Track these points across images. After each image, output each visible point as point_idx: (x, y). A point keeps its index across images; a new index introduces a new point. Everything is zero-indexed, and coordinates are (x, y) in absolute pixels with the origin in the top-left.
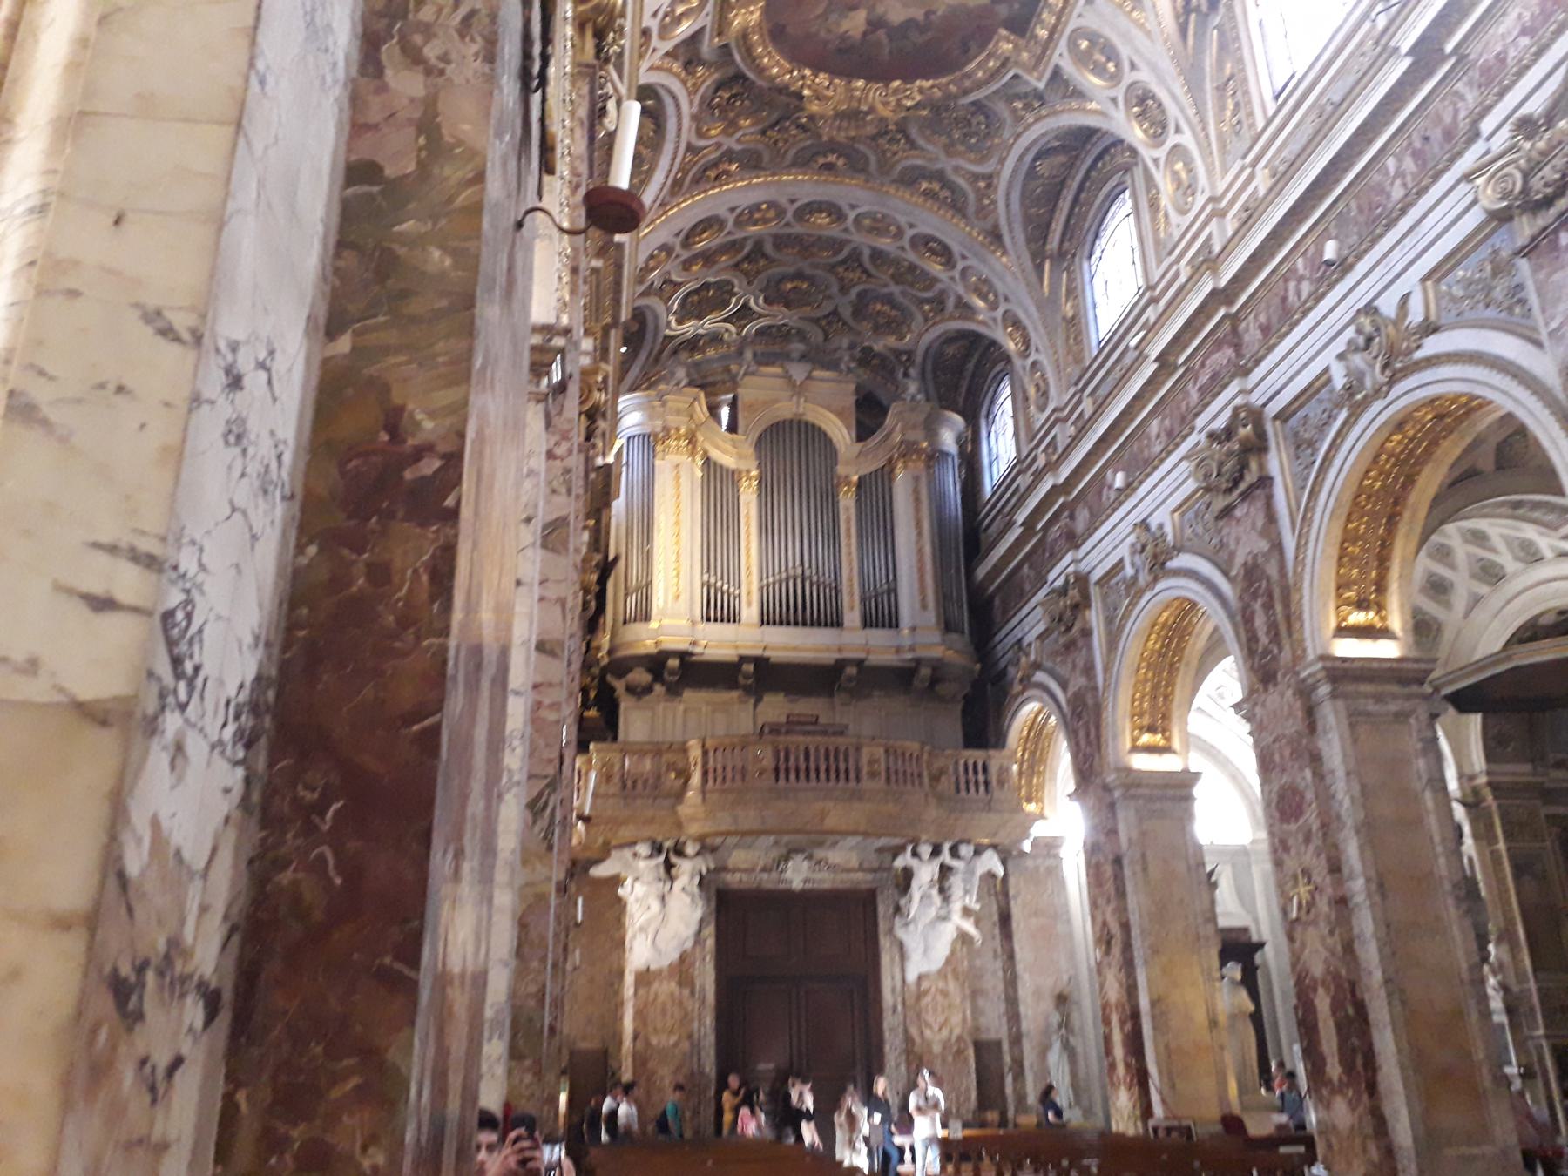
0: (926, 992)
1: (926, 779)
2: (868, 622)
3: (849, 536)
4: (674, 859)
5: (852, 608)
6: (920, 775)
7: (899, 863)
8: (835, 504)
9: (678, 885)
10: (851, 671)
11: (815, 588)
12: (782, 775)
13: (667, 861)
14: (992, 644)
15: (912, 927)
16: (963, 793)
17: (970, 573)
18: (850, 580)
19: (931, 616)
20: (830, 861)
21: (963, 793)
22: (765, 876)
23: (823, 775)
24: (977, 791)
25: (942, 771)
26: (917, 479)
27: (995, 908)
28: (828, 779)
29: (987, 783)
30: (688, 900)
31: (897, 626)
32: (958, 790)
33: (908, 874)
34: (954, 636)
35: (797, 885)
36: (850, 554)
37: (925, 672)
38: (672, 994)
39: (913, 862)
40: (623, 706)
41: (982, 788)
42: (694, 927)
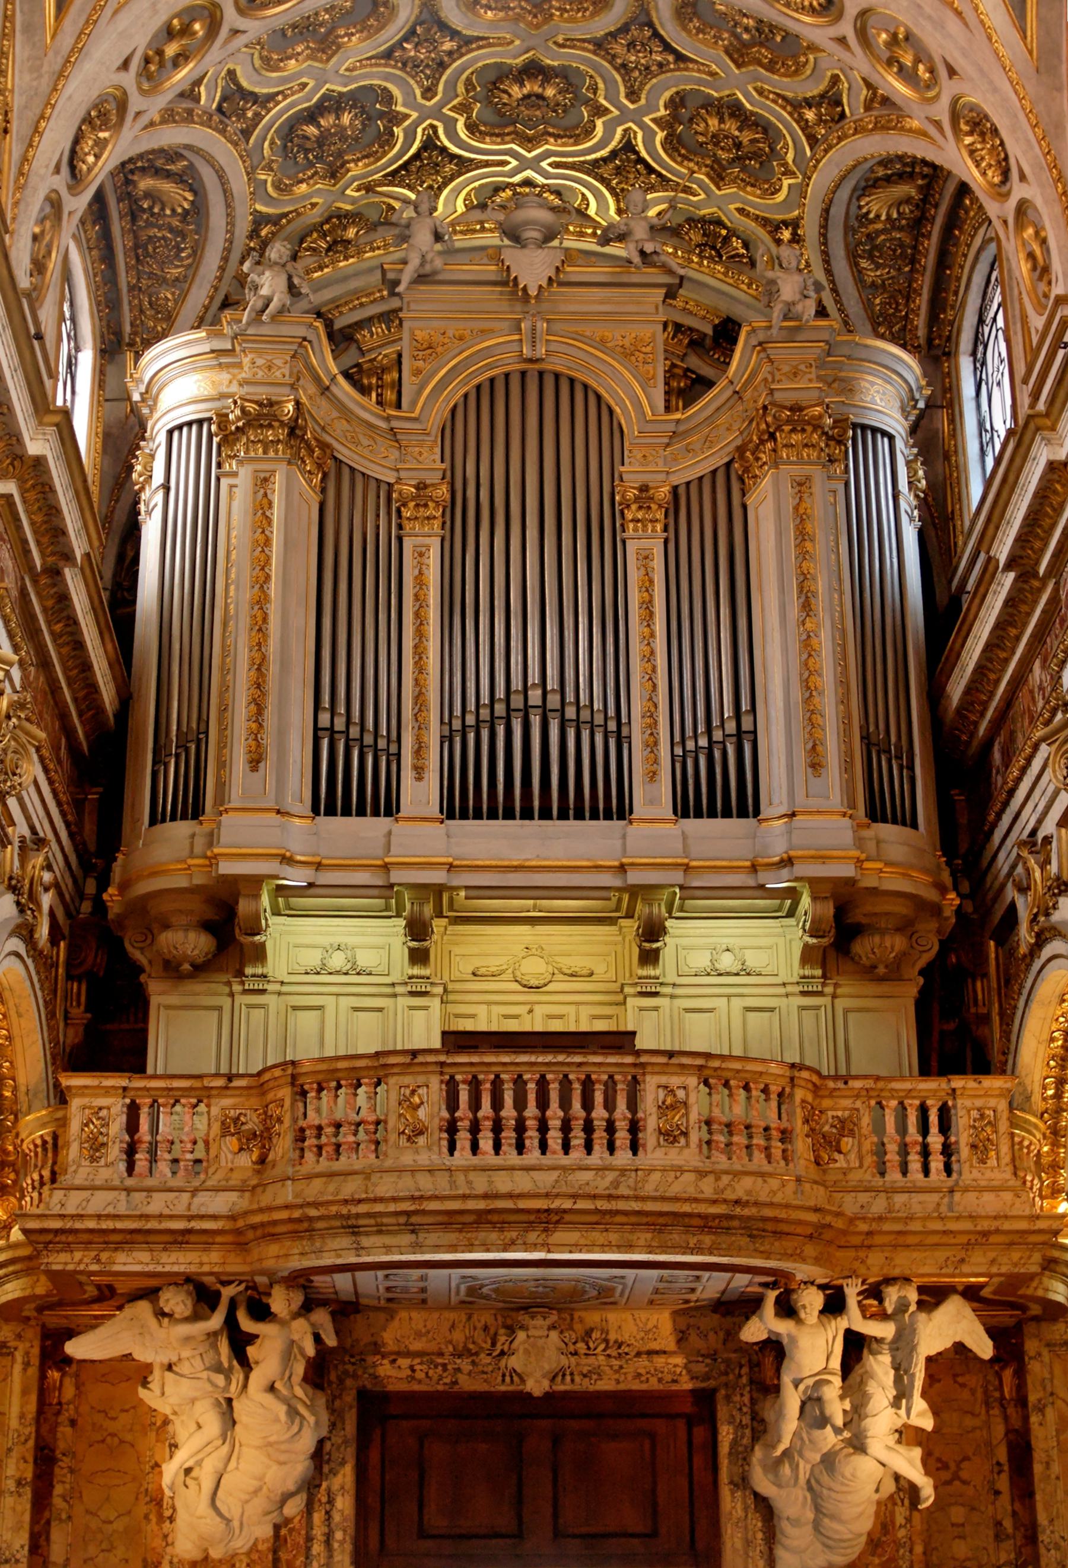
1: (802, 1146)
4: (247, 1324)
5: (653, 776)
6: (786, 1135)
7: (753, 1332)
8: (619, 546)
9: (258, 1378)
11: (571, 734)
12: (463, 1138)
13: (231, 1322)
14: (988, 855)
15: (786, 1470)
16: (894, 1176)
17: (934, 692)
18: (650, 715)
20: (612, 1337)
21: (894, 1176)
22: (465, 1364)
23: (554, 1137)
24: (926, 1171)
25: (846, 1126)
26: (802, 485)
27: (999, 1430)
29: (947, 1150)
30: (281, 1410)
31: (757, 812)
34: (887, 831)
35: (536, 1386)
39: (783, 1327)
40: (154, 1001)
41: (937, 1163)
42: (300, 1467)
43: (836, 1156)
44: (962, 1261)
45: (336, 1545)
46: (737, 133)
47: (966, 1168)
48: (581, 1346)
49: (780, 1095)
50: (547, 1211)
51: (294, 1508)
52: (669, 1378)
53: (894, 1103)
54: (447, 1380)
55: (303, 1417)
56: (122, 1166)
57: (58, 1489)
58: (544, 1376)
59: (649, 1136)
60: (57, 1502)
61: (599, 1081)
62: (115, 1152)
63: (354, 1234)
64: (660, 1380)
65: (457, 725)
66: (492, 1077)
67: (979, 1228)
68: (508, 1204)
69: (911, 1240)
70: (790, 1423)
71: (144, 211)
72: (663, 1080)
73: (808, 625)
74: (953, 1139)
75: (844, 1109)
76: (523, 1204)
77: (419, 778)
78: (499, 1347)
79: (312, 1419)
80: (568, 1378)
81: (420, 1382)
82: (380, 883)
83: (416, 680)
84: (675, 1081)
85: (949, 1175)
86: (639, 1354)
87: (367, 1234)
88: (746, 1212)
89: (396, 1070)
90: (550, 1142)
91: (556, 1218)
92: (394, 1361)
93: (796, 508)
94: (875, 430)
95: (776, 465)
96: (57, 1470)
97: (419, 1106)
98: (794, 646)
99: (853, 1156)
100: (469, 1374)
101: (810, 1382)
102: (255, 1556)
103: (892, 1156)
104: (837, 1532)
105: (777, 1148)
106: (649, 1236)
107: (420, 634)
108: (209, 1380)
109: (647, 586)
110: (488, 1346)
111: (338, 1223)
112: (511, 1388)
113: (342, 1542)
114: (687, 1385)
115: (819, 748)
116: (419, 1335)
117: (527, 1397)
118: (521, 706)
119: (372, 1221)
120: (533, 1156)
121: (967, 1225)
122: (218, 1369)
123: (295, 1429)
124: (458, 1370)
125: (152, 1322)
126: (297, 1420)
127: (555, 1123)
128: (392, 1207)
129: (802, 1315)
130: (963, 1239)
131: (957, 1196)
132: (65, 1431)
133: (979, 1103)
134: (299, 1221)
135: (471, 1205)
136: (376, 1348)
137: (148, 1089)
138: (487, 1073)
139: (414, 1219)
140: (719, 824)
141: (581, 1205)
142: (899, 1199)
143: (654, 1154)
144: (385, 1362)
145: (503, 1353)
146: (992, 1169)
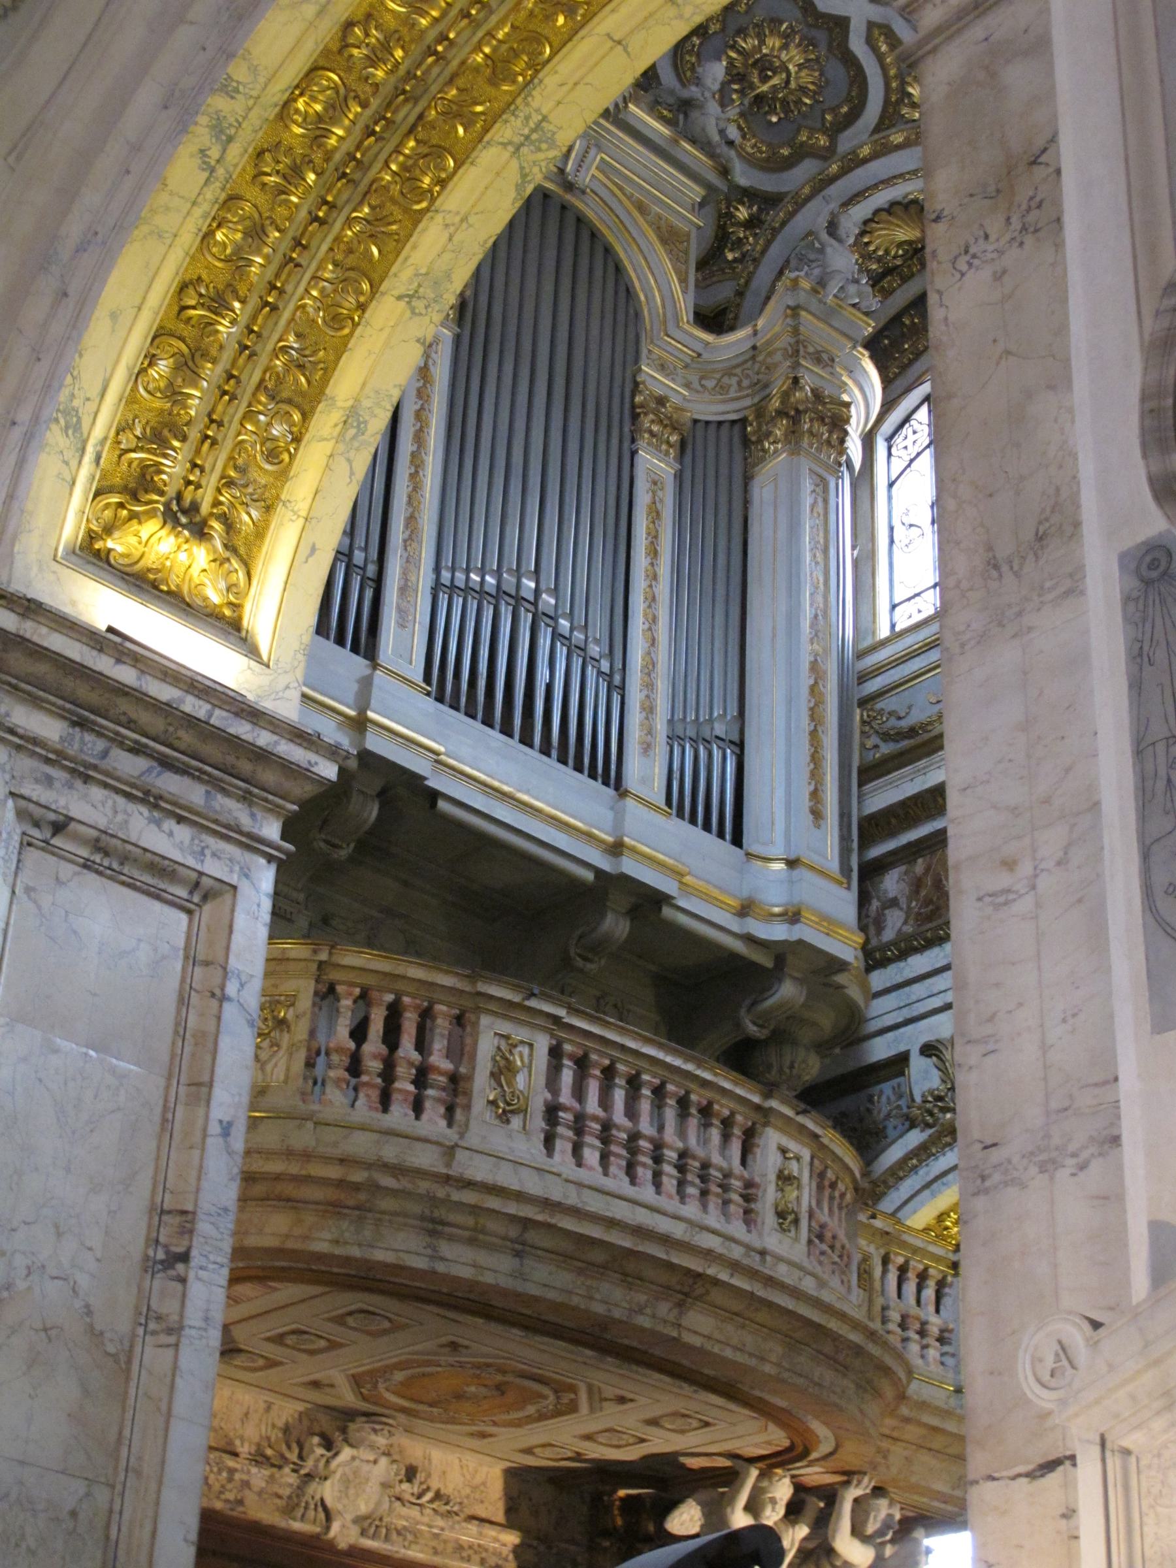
22: (258, 1476)
35: (343, 1533)
36: (652, 600)
37: (788, 991)
50: (699, 1276)
54: (230, 1496)
61: (718, 1114)
63: (433, 1233)
68: (659, 1252)
83: (410, 497)
87: (451, 1238)
89: (493, 1007)
95: (795, 451)
100: (260, 1493)
110: (293, 1456)
111: (417, 1209)
117: (331, 1546)
119: (470, 1221)
124: (246, 1484)
128: (512, 1208)
134: (356, 1187)
138: (602, 1054)
139: (532, 1236)
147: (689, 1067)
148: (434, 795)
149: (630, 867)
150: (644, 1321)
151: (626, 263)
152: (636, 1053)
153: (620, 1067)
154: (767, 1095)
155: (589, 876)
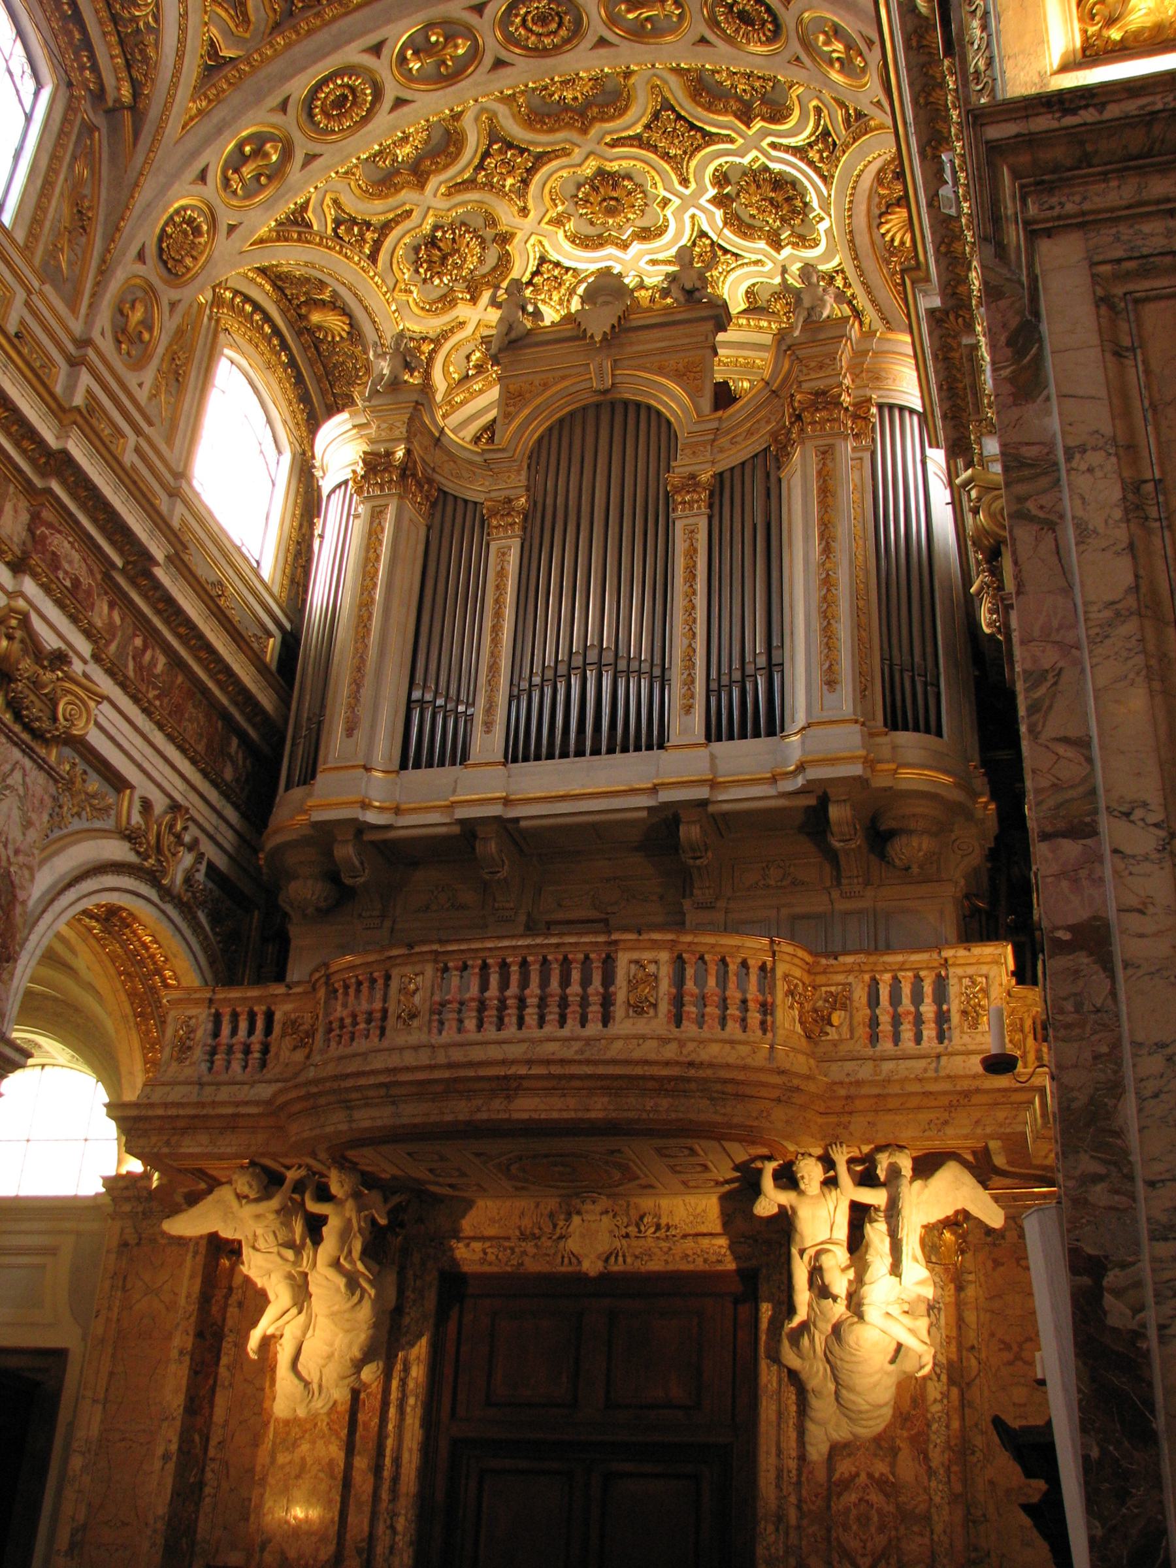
0: (846, 1484)
2: (714, 732)
3: (691, 576)
5: (688, 709)
10: (690, 832)
15: (805, 1341)
16: (886, 1046)
19: (845, 700)
20: (663, 1221)
22: (529, 1247)
23: (531, 1015)
24: (918, 1039)
28: (542, 1022)
29: (942, 1018)
30: (341, 1282)
32: (874, 1039)
33: (784, 1222)
34: (904, 738)
35: (591, 1266)
38: (331, 1463)
39: (785, 1198)
41: (929, 1032)
43: (828, 1029)
44: (946, 1123)
45: (409, 1410)
46: (772, 195)
47: (956, 1034)
48: (632, 1230)
49: (763, 968)
50: (505, 1077)
51: (369, 1373)
52: (714, 1258)
53: (887, 977)
55: (363, 1291)
56: (204, 1067)
57: (224, 1360)
58: (599, 1257)
59: (619, 1010)
60: (223, 1371)
61: (575, 961)
62: (198, 1053)
63: (348, 1108)
64: (705, 1261)
65: (524, 685)
66: (480, 962)
67: (958, 1088)
68: (471, 1073)
69: (892, 1103)
70: (803, 1295)
71: (322, 341)
72: (635, 955)
73: (828, 565)
74: (945, 1007)
75: (838, 984)
76: (483, 1072)
77: (487, 732)
78: (558, 1231)
79: (372, 1292)
80: (620, 1259)
81: (490, 1264)
82: (448, 820)
84: (646, 956)
85: (941, 1042)
86: (685, 1236)
88: (701, 1073)
90: (527, 1018)
91: (514, 1085)
92: (468, 1245)
93: (819, 473)
94: (902, 409)
96: (224, 1344)
97: (415, 992)
98: (815, 583)
99: (845, 1030)
101: (812, 1252)
102: (334, 1417)
103: (885, 1025)
104: (854, 1402)
105: (754, 1017)
106: (606, 1099)
107: (498, 615)
108: (279, 1254)
109: (692, 552)
112: (570, 1269)
113: (414, 1408)
114: (730, 1265)
115: (835, 667)
116: (492, 1221)
117: (581, 1278)
118: (580, 664)
120: (511, 1031)
121: (947, 1086)
122: (290, 1245)
123: (356, 1298)
124: (524, 1253)
125: (234, 1203)
126: (358, 1293)
127: (532, 1001)
129: (802, 1186)
130: (945, 1101)
131: (944, 1060)
132: (233, 1311)
133: (970, 970)
135: (437, 1075)
136: (456, 1234)
137: (230, 1000)
138: (474, 959)
139: (394, 1091)
140: (750, 744)
141: (535, 1070)
142: (887, 1066)
143: (623, 1025)
144: (461, 1245)
145: (561, 1237)
146: (983, 1033)
147: (539, 941)
148: (517, 820)
149: (665, 796)
150: (484, 1116)
151: (660, 407)
152: (514, 947)
153: (490, 961)
154: (609, 933)
155: (644, 814)
